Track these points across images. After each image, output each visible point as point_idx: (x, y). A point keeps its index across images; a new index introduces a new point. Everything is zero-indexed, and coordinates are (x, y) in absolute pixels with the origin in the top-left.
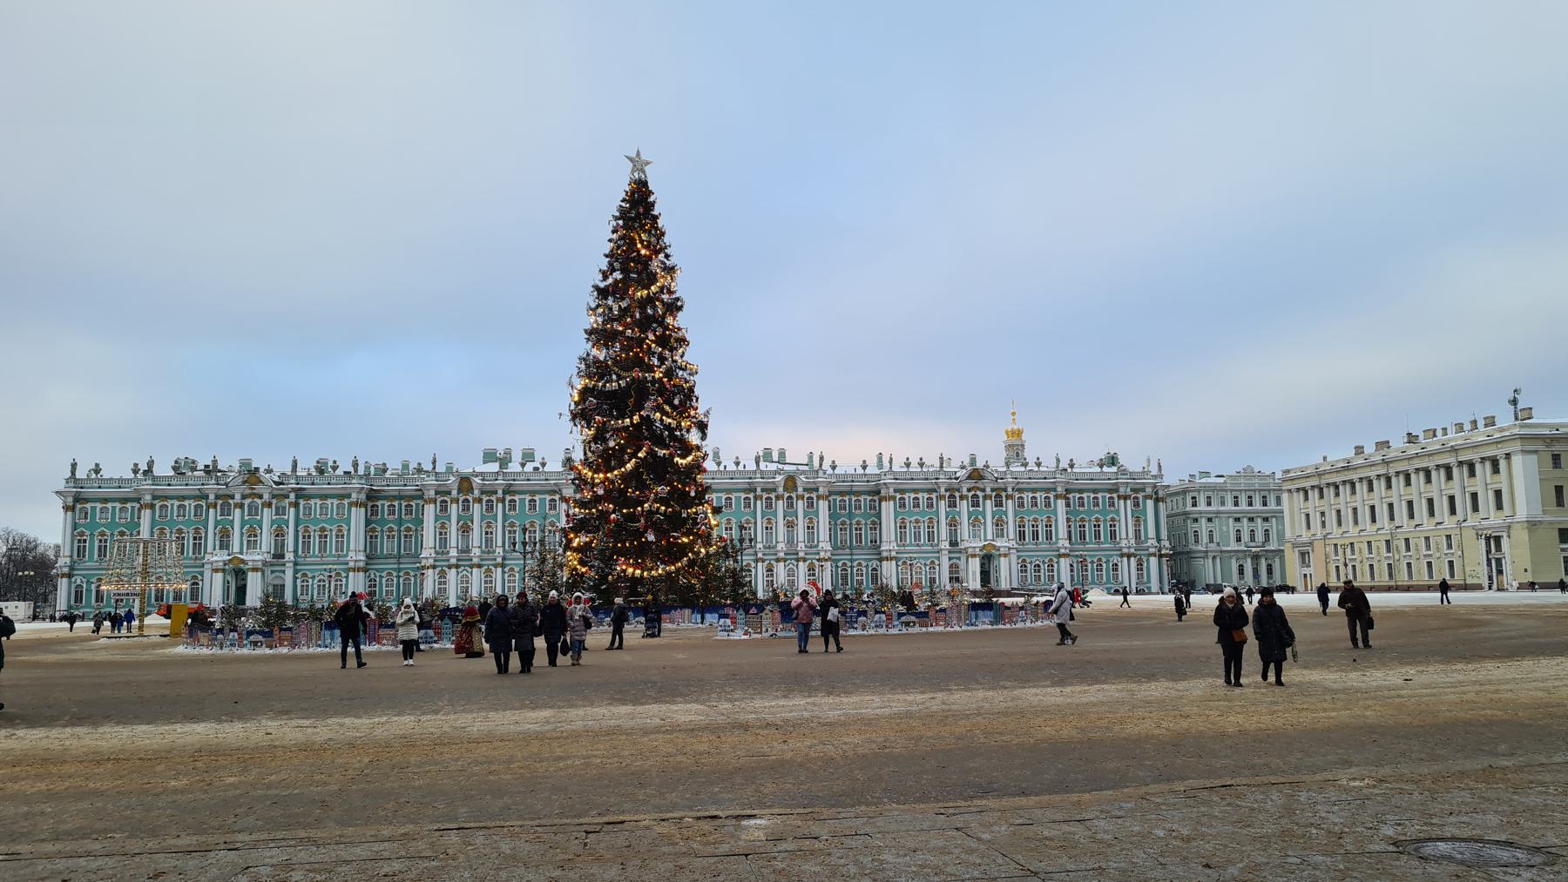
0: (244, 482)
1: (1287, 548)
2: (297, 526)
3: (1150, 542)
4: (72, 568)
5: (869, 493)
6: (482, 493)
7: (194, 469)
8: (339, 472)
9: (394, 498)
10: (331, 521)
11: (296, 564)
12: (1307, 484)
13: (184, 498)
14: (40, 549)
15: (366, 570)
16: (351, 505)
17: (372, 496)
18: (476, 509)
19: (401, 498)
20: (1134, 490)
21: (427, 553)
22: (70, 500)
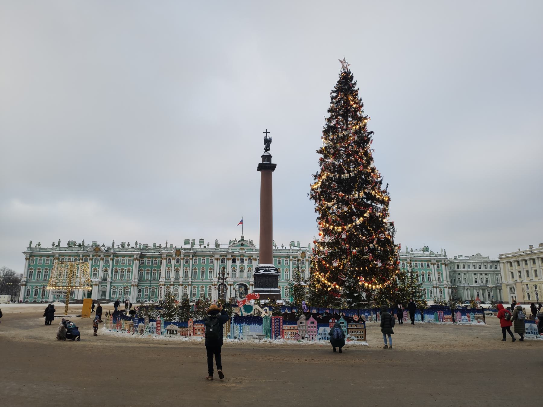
0: (94, 250)
1: (504, 287)
2: (113, 267)
3: (444, 282)
4: (27, 282)
6: (184, 256)
7: (75, 245)
8: (130, 247)
9: (150, 257)
11: (111, 283)
12: (512, 260)
13: (70, 256)
14: (16, 275)
15: (138, 286)
16: (134, 260)
17: (142, 256)
18: (182, 262)
19: (152, 257)
20: (437, 261)
21: (162, 279)
22: (28, 256)
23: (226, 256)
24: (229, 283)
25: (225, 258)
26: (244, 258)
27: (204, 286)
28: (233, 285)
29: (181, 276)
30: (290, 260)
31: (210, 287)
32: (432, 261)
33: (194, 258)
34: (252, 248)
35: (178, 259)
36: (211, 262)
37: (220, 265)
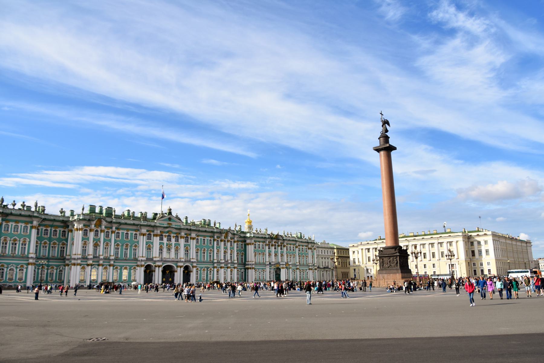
5: (242, 241)
6: (106, 227)
10: (20, 236)
23: (153, 231)
24: (158, 264)
25: (152, 233)
26: (172, 235)
27: (128, 268)
28: (161, 266)
29: (101, 254)
30: (214, 240)
31: (135, 268)
32: (310, 246)
33: (117, 231)
34: (179, 224)
35: (97, 231)
36: (136, 238)
37: (146, 242)
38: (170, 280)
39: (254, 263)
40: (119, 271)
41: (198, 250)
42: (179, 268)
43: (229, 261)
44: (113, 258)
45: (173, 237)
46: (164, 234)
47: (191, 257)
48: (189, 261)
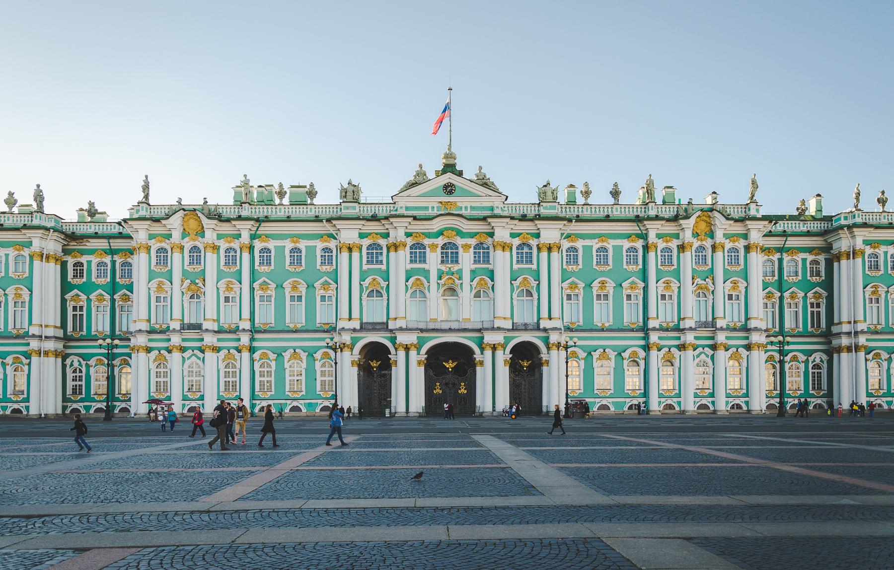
18: (211, 261)
25: (383, 242)
26: (460, 241)
28: (418, 348)
29: (211, 313)
30: (646, 248)
33: (258, 245)
38: (463, 391)
39: (861, 327)
40: (273, 364)
41: (573, 286)
42: (488, 353)
43: (720, 323)
44: (246, 325)
45: (466, 247)
46: (427, 242)
47: (544, 313)
48: (537, 328)
